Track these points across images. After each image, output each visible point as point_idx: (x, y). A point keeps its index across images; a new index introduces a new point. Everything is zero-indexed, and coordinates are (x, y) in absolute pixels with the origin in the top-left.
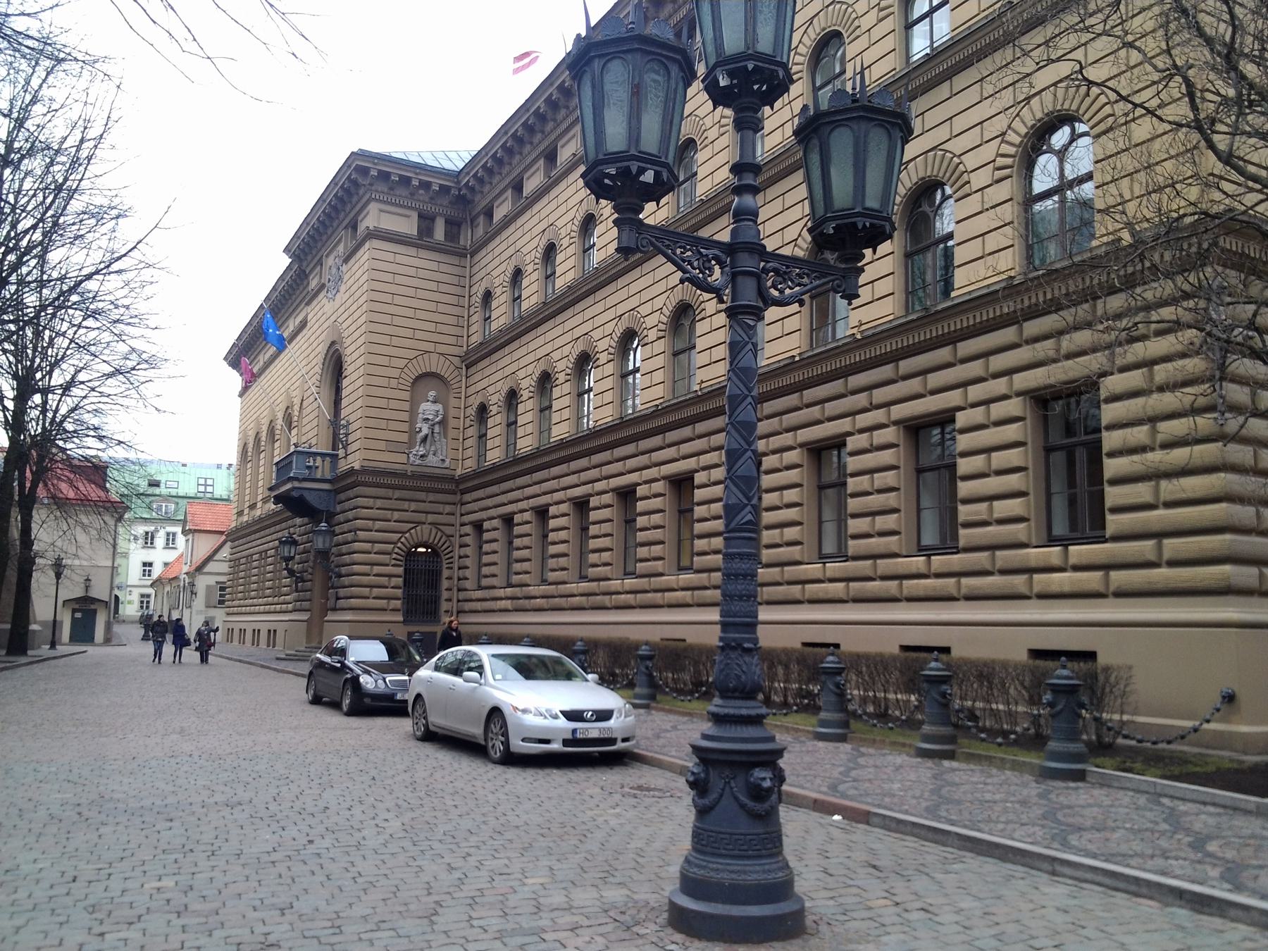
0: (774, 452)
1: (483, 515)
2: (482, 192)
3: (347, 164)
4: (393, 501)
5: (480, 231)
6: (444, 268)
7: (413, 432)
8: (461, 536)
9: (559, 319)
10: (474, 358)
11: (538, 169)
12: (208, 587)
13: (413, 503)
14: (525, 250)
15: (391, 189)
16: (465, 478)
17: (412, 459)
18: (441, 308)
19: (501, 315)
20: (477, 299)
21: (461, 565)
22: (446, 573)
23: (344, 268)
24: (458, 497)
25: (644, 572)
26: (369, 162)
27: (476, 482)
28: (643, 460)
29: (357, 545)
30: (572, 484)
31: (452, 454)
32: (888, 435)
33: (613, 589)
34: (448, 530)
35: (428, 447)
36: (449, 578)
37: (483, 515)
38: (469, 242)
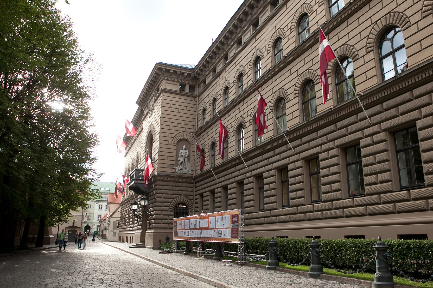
0: (324, 151)
1: (204, 191)
2: (202, 75)
3: (155, 68)
4: (170, 187)
5: (202, 88)
6: (188, 102)
7: (177, 161)
8: (195, 199)
9: (230, 113)
10: (200, 132)
11: (221, 63)
12: (114, 222)
14: (217, 91)
15: (170, 75)
16: (197, 177)
17: (177, 171)
18: (188, 116)
19: (209, 115)
20: (201, 112)
21: (196, 210)
23: (155, 104)
24: (194, 184)
25: (268, 209)
26: (162, 66)
27: (200, 179)
28: (266, 162)
29: (157, 204)
30: (237, 175)
31: (192, 169)
32: (381, 136)
33: (255, 216)
34: (191, 197)
35: (183, 166)
37: (204, 191)
38: (198, 93)
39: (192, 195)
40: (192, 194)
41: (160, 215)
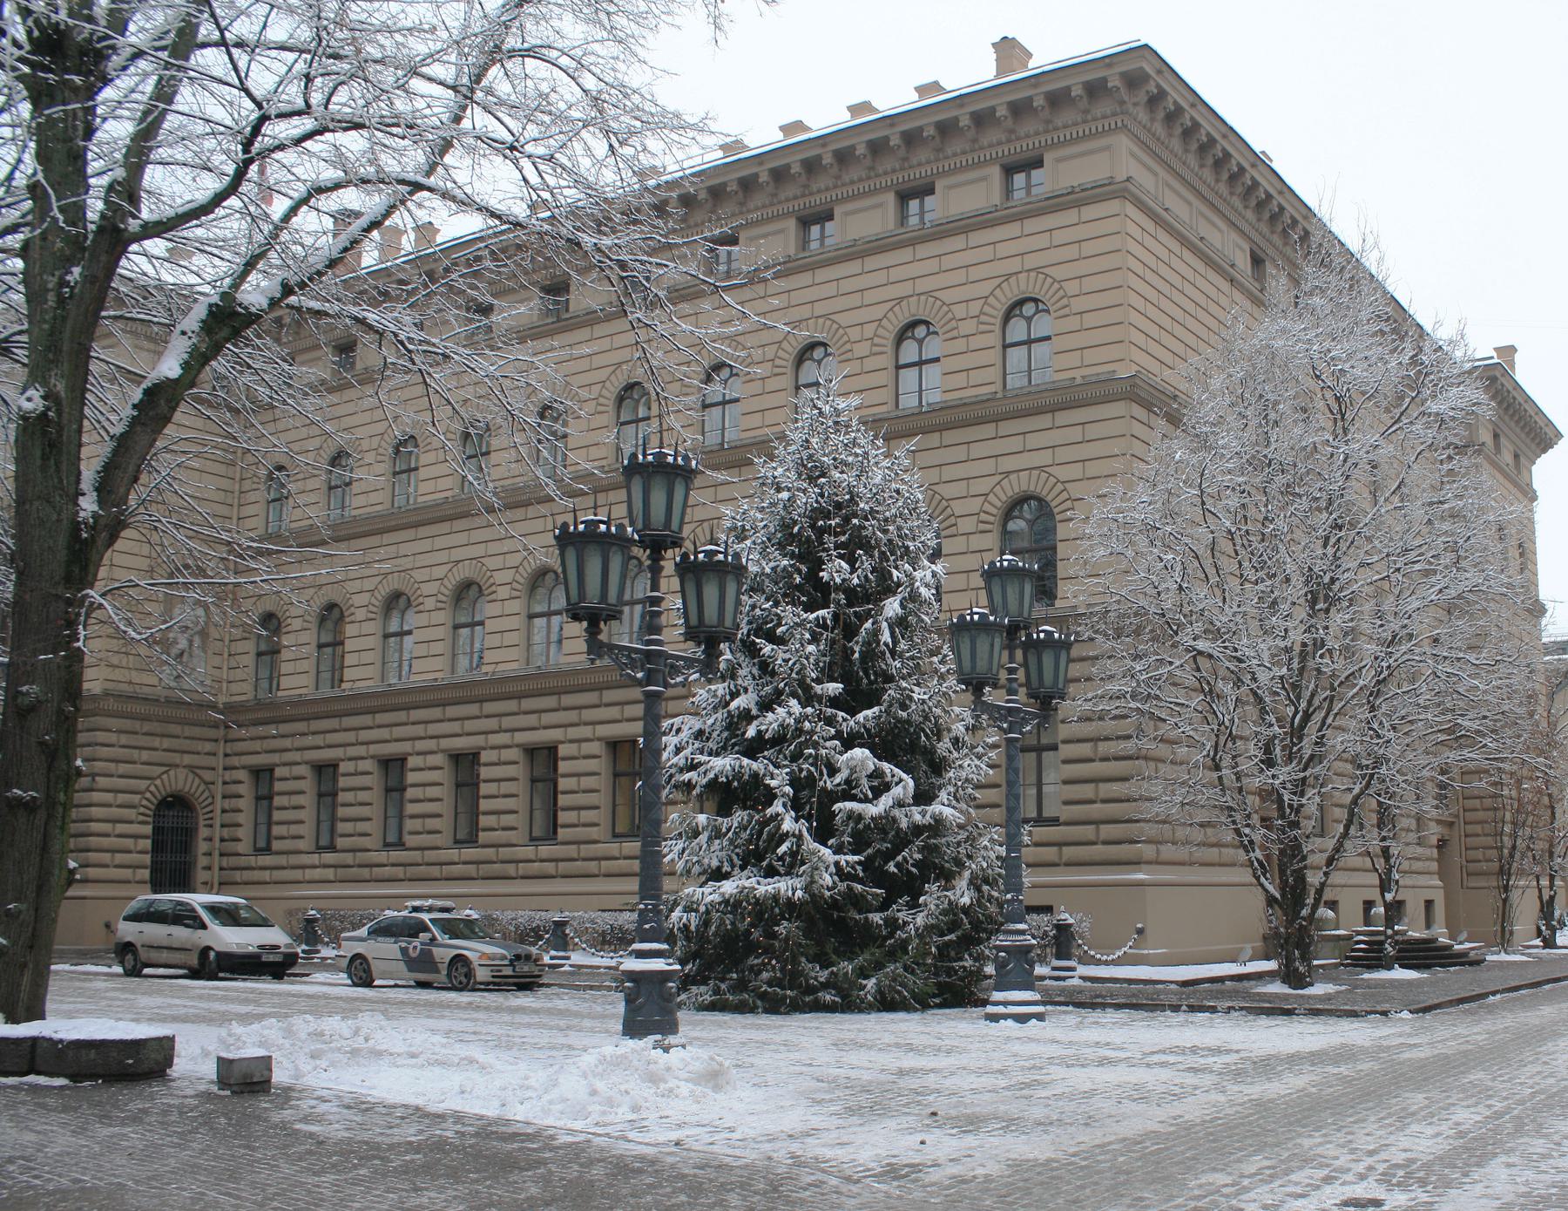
13: (165, 740)
22: (203, 832)
34: (208, 776)
36: (210, 839)
39: (213, 769)
40: (214, 765)
41: (107, 835)
